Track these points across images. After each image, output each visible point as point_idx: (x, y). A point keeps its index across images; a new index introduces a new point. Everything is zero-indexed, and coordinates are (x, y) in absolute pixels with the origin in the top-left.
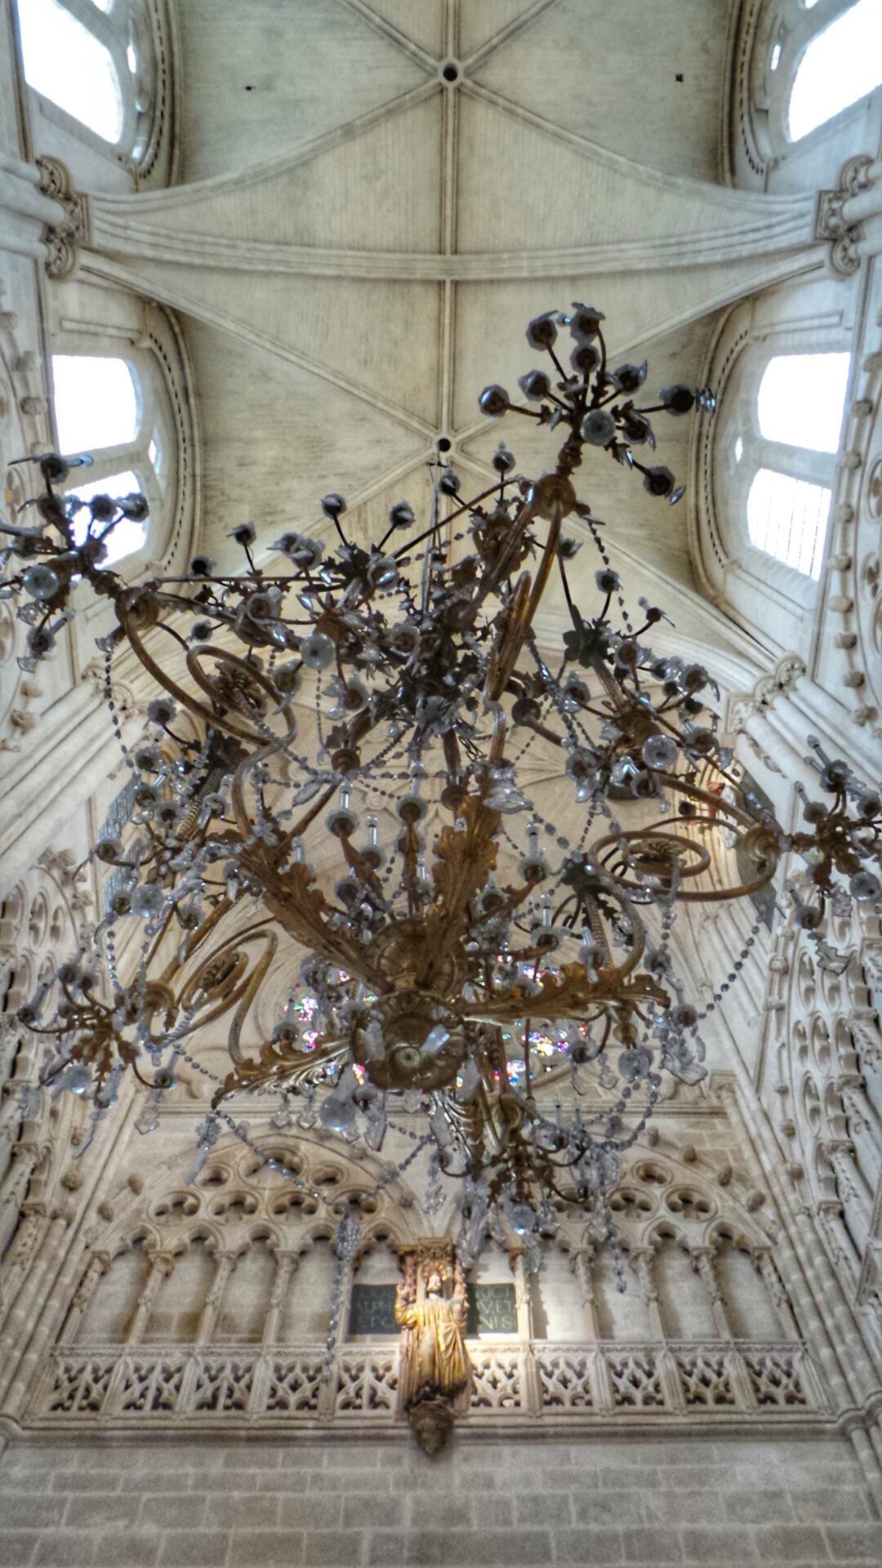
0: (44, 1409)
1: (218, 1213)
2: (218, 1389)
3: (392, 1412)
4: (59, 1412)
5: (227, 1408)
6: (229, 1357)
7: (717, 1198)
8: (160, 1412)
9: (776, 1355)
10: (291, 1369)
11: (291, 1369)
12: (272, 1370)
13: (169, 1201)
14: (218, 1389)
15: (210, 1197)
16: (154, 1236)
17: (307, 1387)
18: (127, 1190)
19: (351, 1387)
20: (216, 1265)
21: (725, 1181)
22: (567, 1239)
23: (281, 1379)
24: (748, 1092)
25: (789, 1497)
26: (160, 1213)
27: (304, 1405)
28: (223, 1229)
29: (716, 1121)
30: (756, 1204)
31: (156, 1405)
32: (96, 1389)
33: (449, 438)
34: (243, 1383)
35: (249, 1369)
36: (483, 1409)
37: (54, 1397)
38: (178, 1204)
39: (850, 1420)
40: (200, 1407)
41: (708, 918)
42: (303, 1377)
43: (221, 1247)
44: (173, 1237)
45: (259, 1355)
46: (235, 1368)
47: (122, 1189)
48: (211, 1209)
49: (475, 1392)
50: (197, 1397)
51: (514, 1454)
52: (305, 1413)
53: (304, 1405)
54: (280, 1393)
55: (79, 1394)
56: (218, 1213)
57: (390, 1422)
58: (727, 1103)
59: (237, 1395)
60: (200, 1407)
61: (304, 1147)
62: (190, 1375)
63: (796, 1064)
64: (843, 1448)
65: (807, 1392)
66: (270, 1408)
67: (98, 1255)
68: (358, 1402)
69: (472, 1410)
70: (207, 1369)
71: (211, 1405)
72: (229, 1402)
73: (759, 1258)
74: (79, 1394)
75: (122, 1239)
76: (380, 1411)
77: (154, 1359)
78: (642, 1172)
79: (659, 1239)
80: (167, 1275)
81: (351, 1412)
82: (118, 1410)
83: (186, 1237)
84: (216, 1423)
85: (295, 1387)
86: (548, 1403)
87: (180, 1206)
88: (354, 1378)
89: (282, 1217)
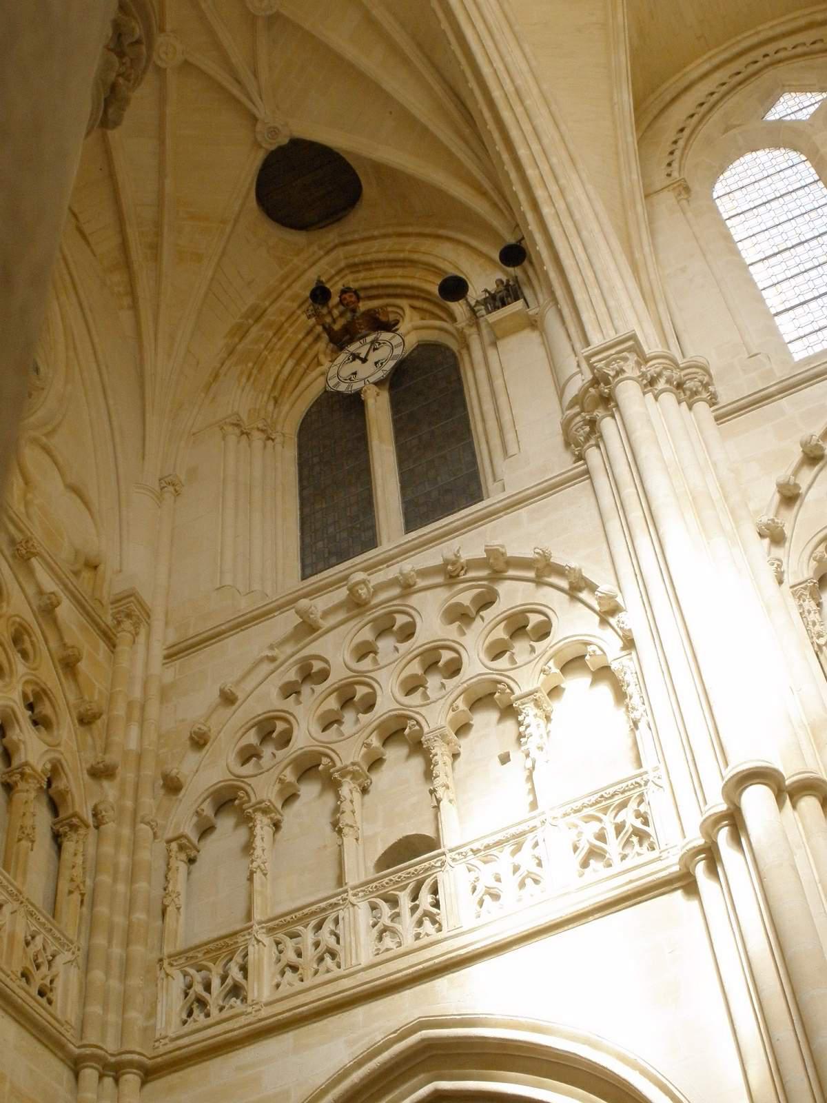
7: (66, 729)
9: (50, 939)
21: (86, 720)
24: (158, 651)
25: (7, 1086)
29: (102, 645)
30: (101, 773)
39: (93, 1057)
41: (237, 425)
58: (124, 637)
63: (272, 691)
64: (66, 1074)
65: (57, 996)
73: (74, 828)
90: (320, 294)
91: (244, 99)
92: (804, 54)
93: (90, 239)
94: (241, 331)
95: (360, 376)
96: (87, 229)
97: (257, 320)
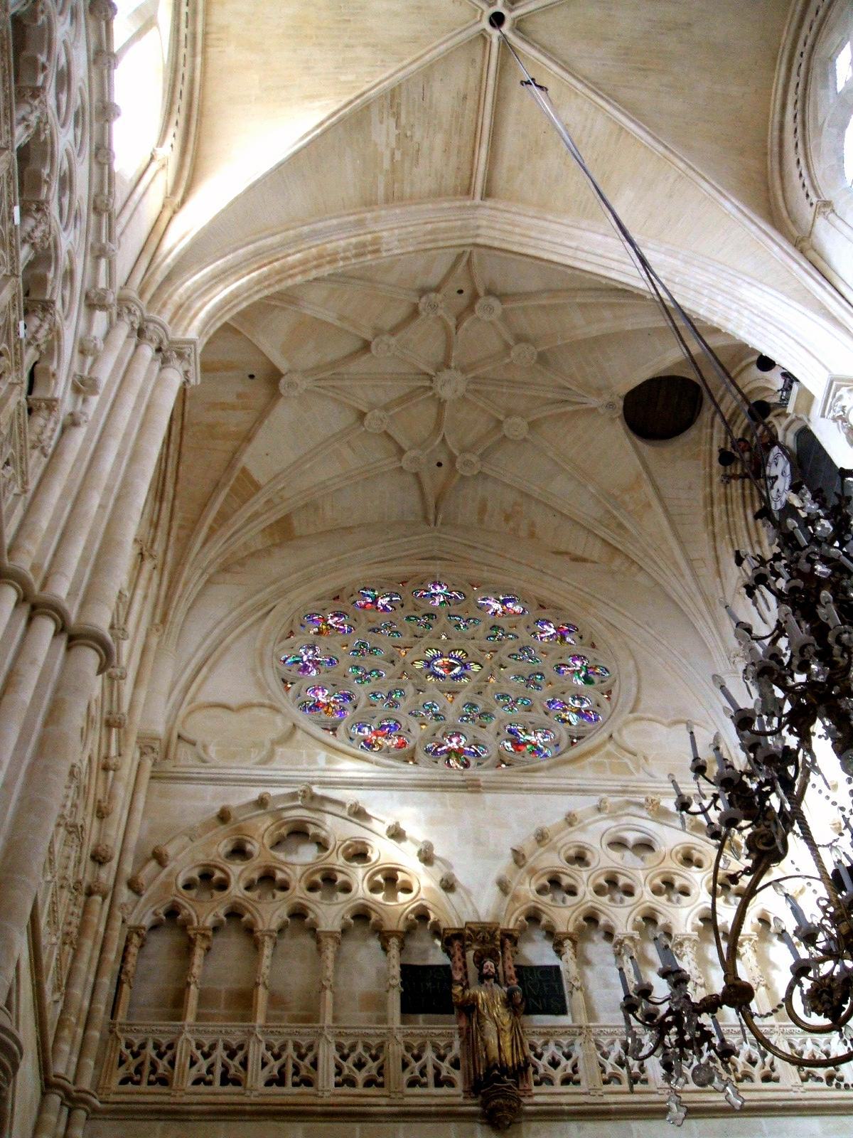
0: (114, 1084)
1: (248, 888)
2: (283, 1066)
3: (459, 1089)
4: (130, 1086)
5: (295, 1084)
6: (291, 1034)
8: (230, 1088)
10: (353, 1048)
11: (353, 1048)
12: (334, 1047)
13: (195, 874)
14: (283, 1066)
15: (238, 872)
16: (188, 910)
17: (372, 1066)
18: (153, 863)
19: (416, 1066)
20: (256, 946)
22: (612, 924)
23: (344, 1057)
26: (188, 886)
27: (369, 1083)
28: (259, 906)
31: (225, 1080)
32: (162, 1065)
33: (505, 12)
34: (307, 1061)
35: (310, 1048)
36: (545, 1088)
37: (121, 1073)
38: (206, 876)
40: (269, 1083)
42: (367, 1055)
43: (260, 926)
44: (208, 912)
45: (321, 1035)
46: (297, 1046)
47: (148, 860)
48: (242, 885)
49: (536, 1072)
50: (264, 1075)
51: (580, 1129)
52: (373, 1090)
53: (369, 1083)
54: (346, 1072)
55: (147, 1068)
56: (248, 888)
57: (460, 1100)
59: (303, 1072)
60: (269, 1083)
61: (329, 820)
62: (256, 1052)
66: (337, 1085)
67: (136, 930)
68: (424, 1080)
69: (535, 1089)
70: (269, 1047)
71: (279, 1080)
72: (297, 1079)
74: (147, 1068)
75: (155, 913)
76: (445, 1090)
77: (215, 1037)
78: (680, 856)
79: (701, 924)
80: (208, 949)
81: (417, 1090)
82: (188, 1084)
83: (221, 913)
84: (290, 1099)
85: (360, 1065)
86: (606, 1082)
87: (209, 880)
88: (417, 1058)
89: (317, 896)
90: (726, 458)
91: (577, 407)
92: (821, 25)
93: (586, 555)
94: (710, 519)
95: (781, 490)
96: (579, 553)
97: (712, 504)
